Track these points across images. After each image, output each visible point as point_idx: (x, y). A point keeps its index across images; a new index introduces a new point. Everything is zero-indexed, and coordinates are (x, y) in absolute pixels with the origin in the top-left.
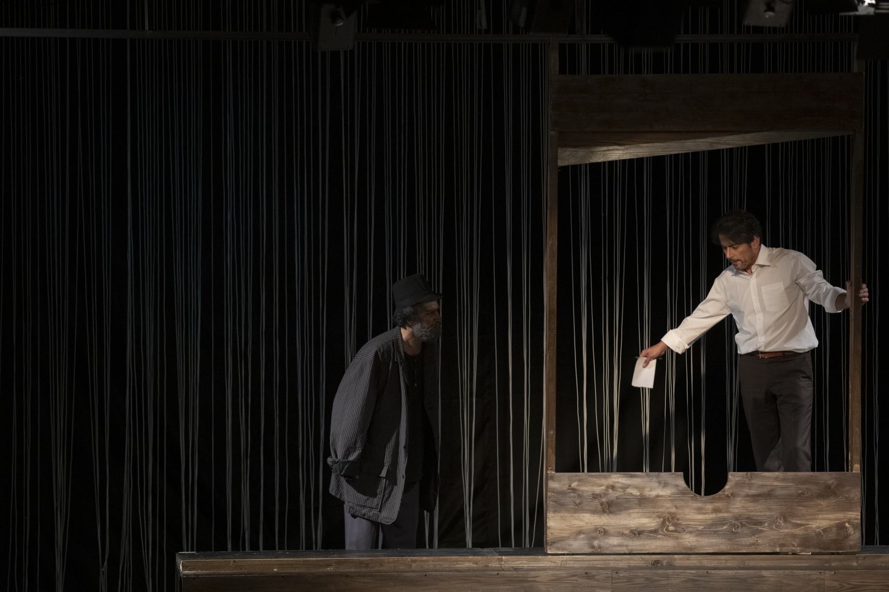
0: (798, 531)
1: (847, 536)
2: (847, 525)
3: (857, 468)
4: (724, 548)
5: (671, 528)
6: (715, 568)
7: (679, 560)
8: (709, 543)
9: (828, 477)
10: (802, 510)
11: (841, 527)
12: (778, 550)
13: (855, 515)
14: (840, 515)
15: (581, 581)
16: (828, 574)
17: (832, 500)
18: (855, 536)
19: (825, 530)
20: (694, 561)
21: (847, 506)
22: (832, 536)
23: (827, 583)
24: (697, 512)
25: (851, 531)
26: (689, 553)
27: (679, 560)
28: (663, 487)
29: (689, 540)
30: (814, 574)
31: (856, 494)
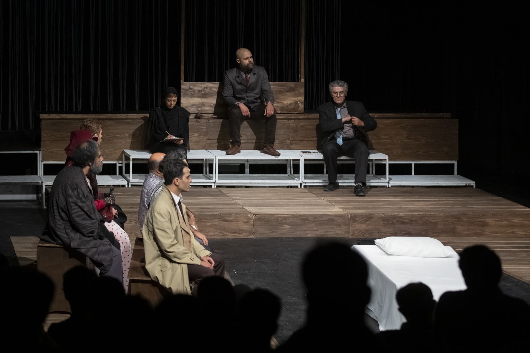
0: (279, 105)
1: (298, 107)
10: (281, 97)
11: (296, 103)
13: (302, 98)
14: (296, 99)
15: (194, 123)
16: (291, 121)
17: (293, 93)
18: (302, 106)
19: (290, 104)
21: (299, 95)
22: (293, 106)
23: (291, 124)
25: (300, 105)
30: (286, 121)
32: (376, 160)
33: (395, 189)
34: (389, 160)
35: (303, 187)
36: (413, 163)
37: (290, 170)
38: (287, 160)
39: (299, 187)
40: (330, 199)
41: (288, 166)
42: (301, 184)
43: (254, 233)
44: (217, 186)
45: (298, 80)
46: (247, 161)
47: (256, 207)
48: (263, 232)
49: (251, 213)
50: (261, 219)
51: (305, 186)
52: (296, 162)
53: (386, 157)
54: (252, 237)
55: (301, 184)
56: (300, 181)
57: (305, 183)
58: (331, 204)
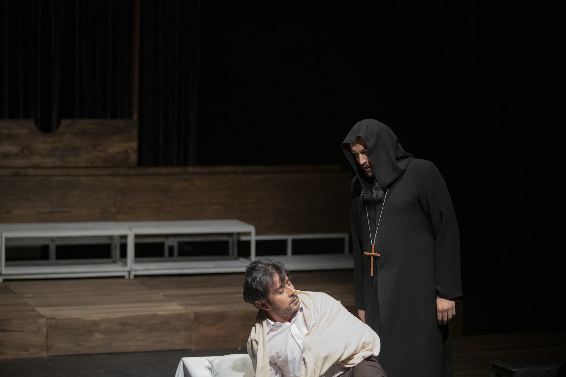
2: (130, 151)
3: (136, 117)
4: (58, 163)
5: (27, 152)
6: (53, 176)
7: (30, 172)
8: (49, 162)
9: (119, 123)
11: (126, 152)
12: (89, 165)
13: (134, 145)
18: (134, 157)
20: (39, 172)
24: (42, 144)
26: (37, 167)
27: (30, 172)
28: (23, 129)
29: (37, 160)
31: (135, 132)
32: (239, 234)
34: (257, 233)
35: (132, 277)
37: (117, 252)
38: (111, 237)
40: (168, 292)
41: (113, 247)
42: (129, 272)
43: (48, 349)
44: (4, 280)
45: (130, 117)
46: (53, 239)
47: (53, 308)
48: (63, 346)
49: (42, 317)
50: (59, 328)
51: (136, 276)
52: (123, 241)
53: (251, 229)
54: (44, 354)
55: (129, 272)
56: (128, 268)
57: (136, 271)
58: (169, 299)
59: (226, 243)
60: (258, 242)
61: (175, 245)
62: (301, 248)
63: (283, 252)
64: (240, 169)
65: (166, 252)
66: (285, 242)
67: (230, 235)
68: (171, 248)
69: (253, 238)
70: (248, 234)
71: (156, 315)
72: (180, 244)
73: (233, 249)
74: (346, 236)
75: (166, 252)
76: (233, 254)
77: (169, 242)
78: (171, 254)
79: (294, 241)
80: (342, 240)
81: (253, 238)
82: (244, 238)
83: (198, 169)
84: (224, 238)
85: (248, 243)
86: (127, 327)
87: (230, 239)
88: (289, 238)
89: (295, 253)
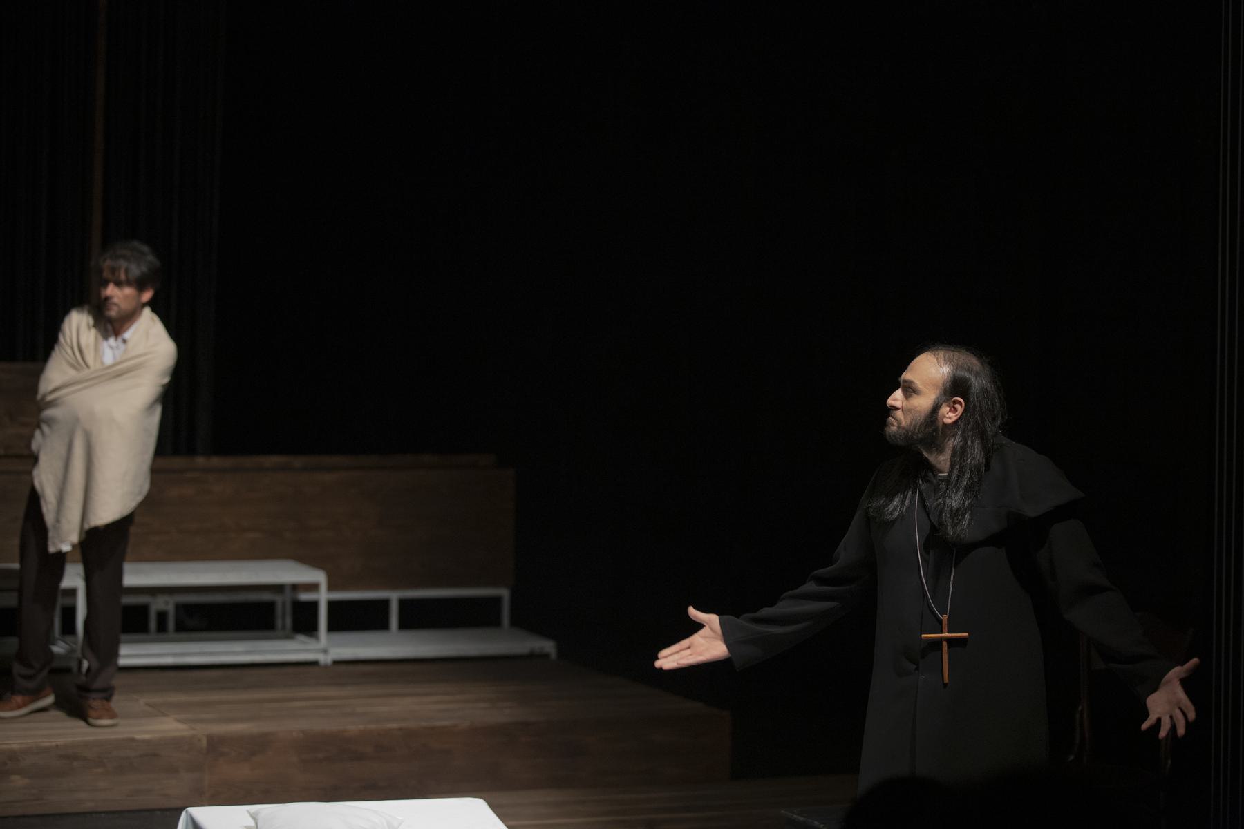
32: (295, 587)
33: (343, 668)
34: (331, 587)
36: (394, 596)
39: (75, 669)
40: (157, 699)
53: (319, 577)
58: (159, 711)
59: (271, 606)
60: (332, 605)
61: (171, 609)
62: (417, 617)
63: (383, 625)
64: (298, 461)
65: (153, 624)
66: (385, 603)
67: (278, 588)
68: (162, 616)
69: (323, 597)
70: (314, 587)
71: (133, 740)
72: (179, 607)
73: (285, 619)
74: (504, 593)
75: (153, 624)
76: (284, 627)
77: (159, 604)
78: (162, 627)
79: (403, 603)
80: (497, 600)
81: (323, 597)
82: (305, 597)
83: (216, 461)
84: (266, 597)
85: (314, 605)
86: (75, 764)
87: (278, 599)
88: (394, 596)
89: (404, 625)
